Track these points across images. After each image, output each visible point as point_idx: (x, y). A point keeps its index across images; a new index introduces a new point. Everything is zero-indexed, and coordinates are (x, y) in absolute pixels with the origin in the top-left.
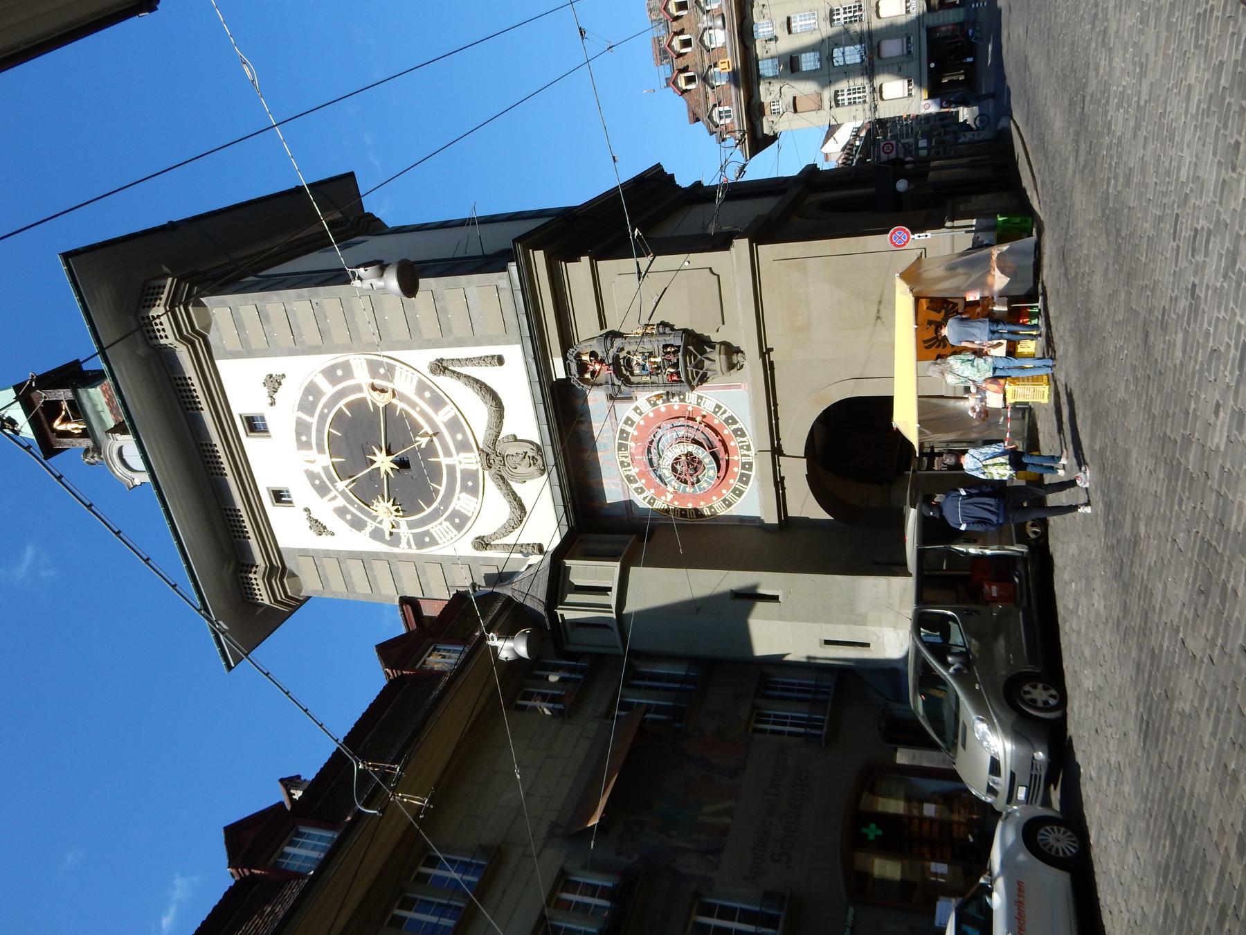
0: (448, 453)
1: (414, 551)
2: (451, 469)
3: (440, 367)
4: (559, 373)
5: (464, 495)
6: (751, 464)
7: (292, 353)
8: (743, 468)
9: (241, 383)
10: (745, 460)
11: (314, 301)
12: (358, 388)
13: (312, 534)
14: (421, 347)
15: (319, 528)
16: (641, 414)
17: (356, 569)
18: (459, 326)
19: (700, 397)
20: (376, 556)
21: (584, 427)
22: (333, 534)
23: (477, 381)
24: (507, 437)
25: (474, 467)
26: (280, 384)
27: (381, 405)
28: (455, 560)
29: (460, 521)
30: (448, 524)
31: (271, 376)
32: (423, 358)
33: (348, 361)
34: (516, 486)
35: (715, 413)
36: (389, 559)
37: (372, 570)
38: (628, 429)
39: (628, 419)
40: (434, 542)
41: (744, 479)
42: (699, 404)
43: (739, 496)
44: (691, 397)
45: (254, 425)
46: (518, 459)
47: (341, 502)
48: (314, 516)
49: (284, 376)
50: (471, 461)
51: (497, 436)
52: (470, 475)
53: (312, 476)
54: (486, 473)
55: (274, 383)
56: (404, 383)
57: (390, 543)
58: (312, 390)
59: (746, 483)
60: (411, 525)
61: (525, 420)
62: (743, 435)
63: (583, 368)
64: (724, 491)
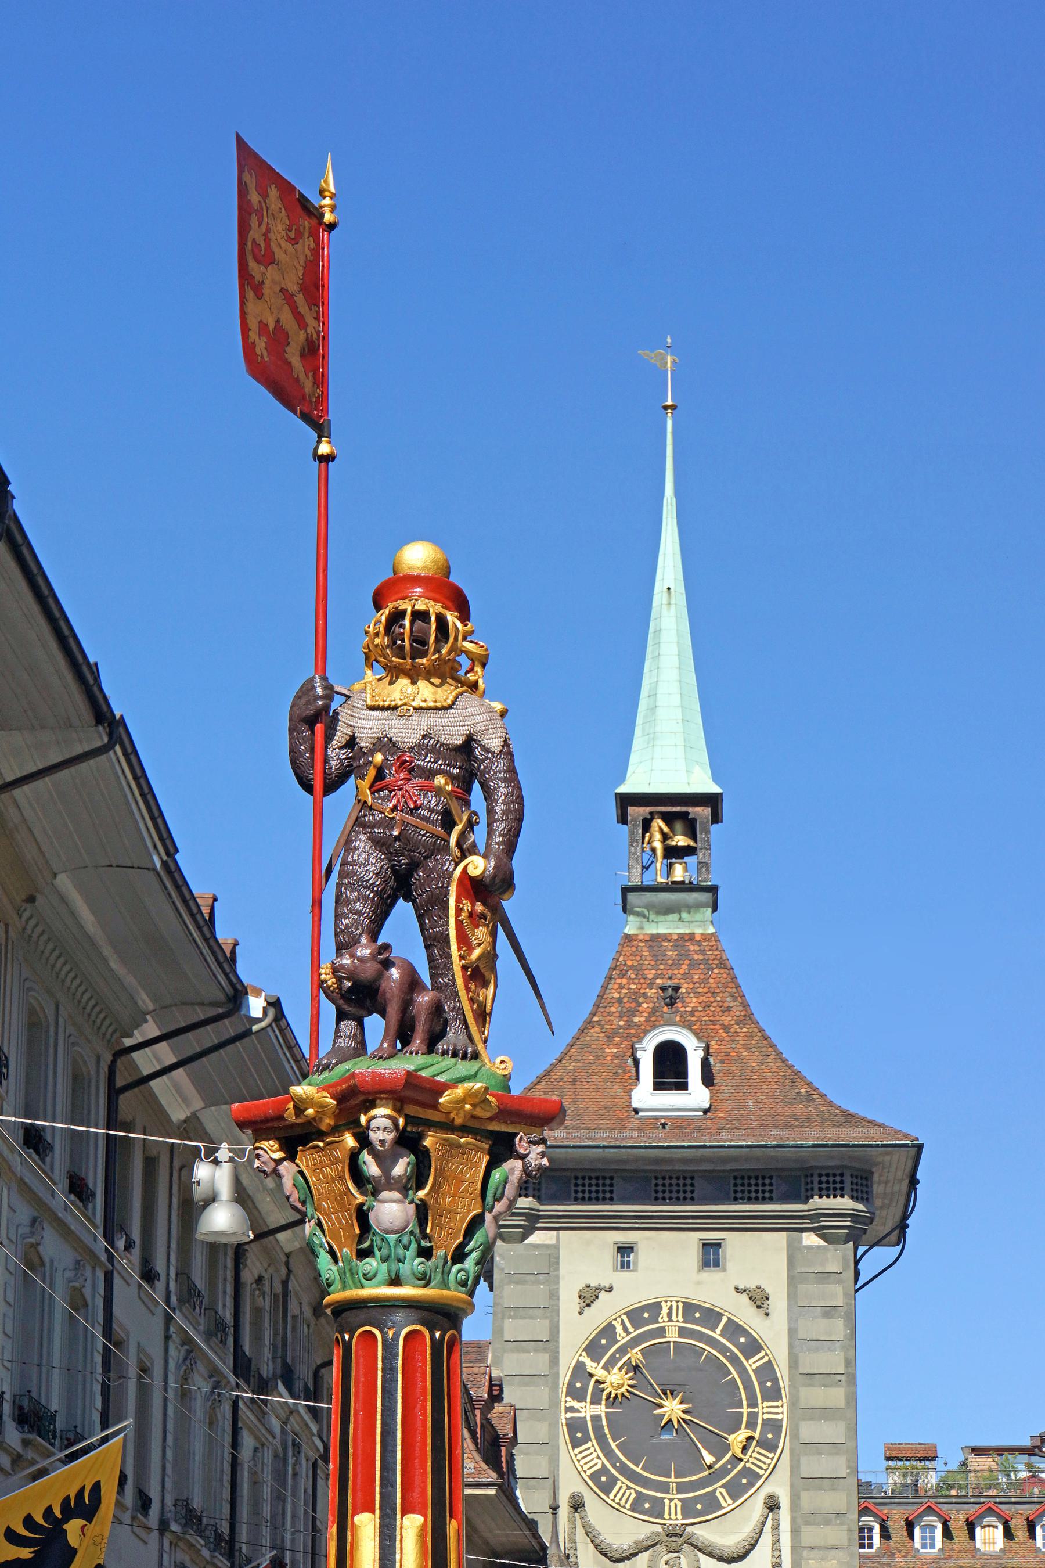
0: (681, 1488)
1: (564, 1416)
2: (665, 1488)
3: (772, 1506)
7: (792, 1332)
9: (759, 1256)
11: (843, 1378)
12: (753, 1404)
14: (792, 1486)
15: (588, 1297)
17: (539, 1329)
18: (810, 1535)
20: (555, 1361)
23: (757, 1541)
26: (759, 1307)
28: (554, 1462)
30: (599, 1466)
31: (768, 1299)
32: (779, 1486)
33: (779, 1397)
36: (550, 1377)
37: (536, 1351)
40: (575, 1443)
45: (711, 1255)
47: (622, 1338)
48: (603, 1295)
49: (767, 1314)
50: (674, 1516)
51: (700, 1550)
52: (657, 1510)
53: (655, 1308)
54: (659, 1529)
55: (759, 1300)
57: (571, 1386)
58: (753, 1347)
60: (596, 1419)
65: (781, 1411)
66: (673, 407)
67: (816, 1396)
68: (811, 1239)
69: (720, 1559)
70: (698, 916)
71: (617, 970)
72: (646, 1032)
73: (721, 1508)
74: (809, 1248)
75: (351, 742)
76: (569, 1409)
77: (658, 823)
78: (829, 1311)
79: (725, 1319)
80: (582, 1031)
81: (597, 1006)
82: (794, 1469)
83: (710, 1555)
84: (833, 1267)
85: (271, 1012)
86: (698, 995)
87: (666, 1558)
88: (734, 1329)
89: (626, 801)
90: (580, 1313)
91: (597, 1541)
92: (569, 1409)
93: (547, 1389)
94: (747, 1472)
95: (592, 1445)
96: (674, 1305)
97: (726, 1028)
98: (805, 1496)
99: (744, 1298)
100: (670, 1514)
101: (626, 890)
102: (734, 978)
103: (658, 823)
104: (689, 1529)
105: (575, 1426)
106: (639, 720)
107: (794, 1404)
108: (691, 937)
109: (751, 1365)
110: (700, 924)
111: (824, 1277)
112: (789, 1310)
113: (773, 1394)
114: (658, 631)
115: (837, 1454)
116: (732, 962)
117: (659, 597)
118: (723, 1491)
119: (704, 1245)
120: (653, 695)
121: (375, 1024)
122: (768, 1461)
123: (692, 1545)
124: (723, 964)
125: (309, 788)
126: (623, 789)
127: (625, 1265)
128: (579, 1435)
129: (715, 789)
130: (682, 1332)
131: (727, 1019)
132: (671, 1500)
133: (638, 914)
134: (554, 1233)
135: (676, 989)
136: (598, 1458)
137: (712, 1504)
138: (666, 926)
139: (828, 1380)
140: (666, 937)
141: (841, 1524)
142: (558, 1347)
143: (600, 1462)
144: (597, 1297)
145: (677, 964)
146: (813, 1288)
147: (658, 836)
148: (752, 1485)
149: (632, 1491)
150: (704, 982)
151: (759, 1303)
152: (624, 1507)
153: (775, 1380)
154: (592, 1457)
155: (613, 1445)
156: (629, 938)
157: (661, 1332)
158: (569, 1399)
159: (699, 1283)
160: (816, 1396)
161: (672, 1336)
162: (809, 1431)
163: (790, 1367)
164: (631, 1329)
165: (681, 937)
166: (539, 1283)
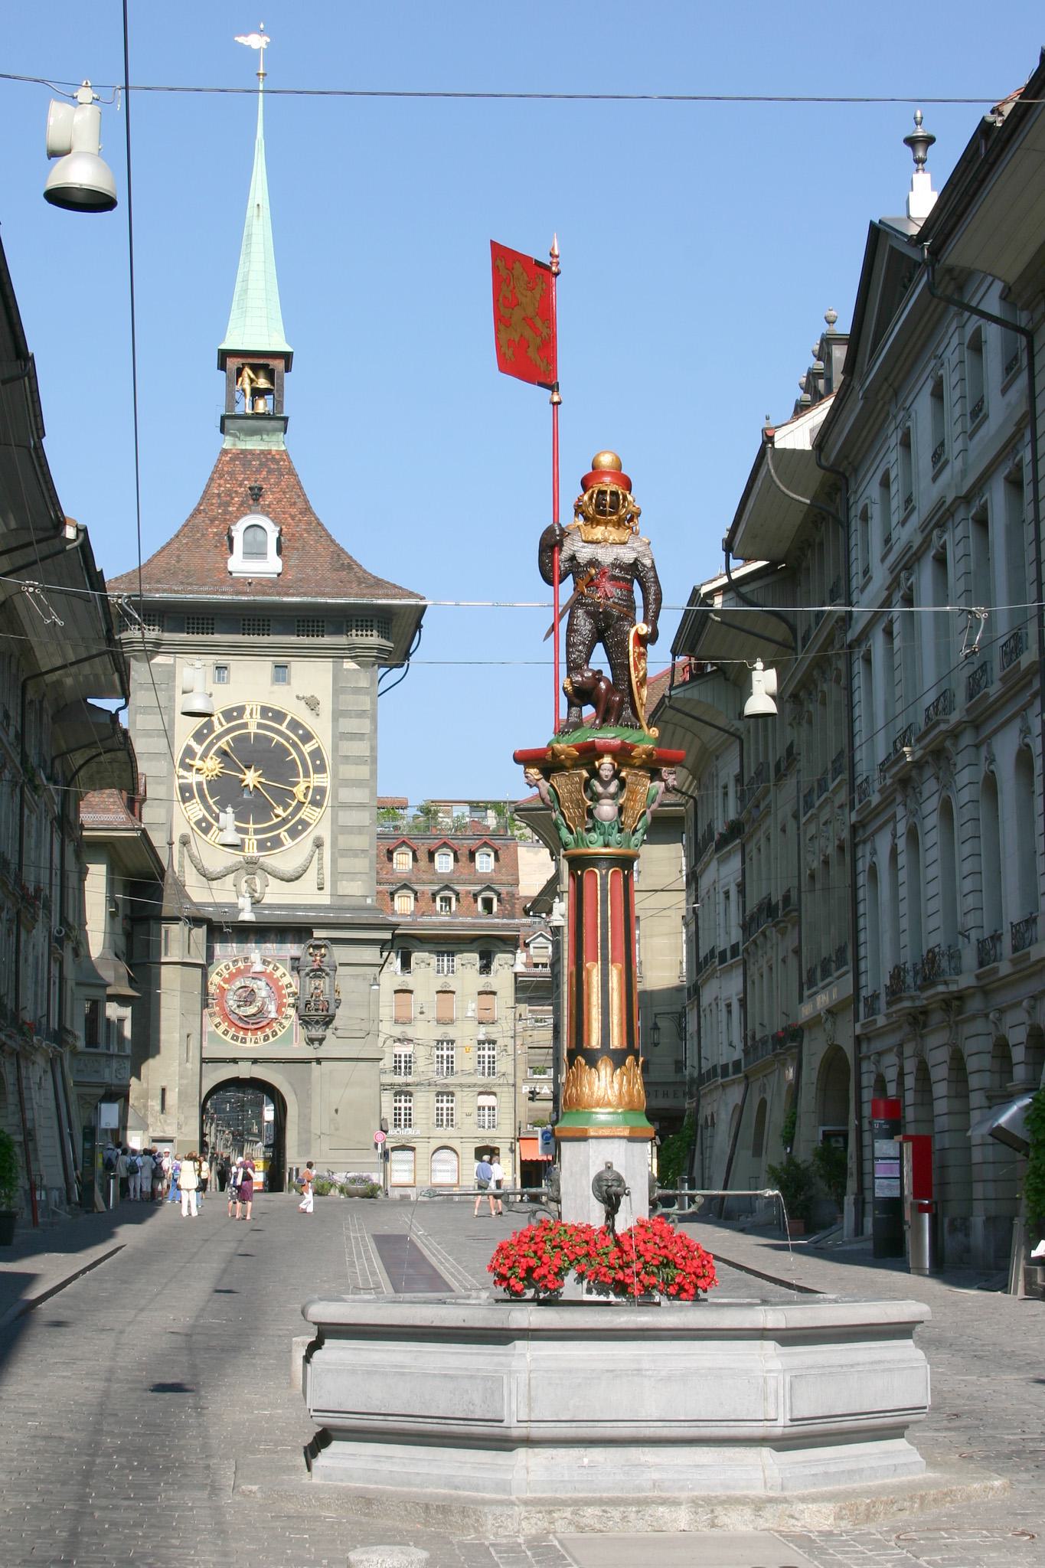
0: (257, 832)
1: (177, 782)
4: (317, 934)
14: (332, 832)
18: (344, 864)
20: (170, 746)
21: (273, 937)
27: (295, 790)
29: (204, 826)
32: (324, 831)
33: (325, 771)
34: (231, 877)
41: (235, 1038)
44: (292, 1012)
47: (218, 729)
50: (251, 851)
53: (241, 710)
55: (312, 704)
58: (307, 737)
63: (318, 947)
65: (324, 780)
66: (264, 75)
67: (350, 771)
68: (350, 665)
69: (282, 879)
70: (274, 438)
71: (218, 473)
72: (238, 518)
73: (283, 845)
75: (573, 558)
77: (247, 371)
78: (361, 714)
79: (288, 718)
80: (192, 516)
81: (203, 498)
82: (334, 820)
84: (364, 683)
85: (82, 535)
86: (273, 493)
88: (295, 725)
89: (224, 355)
94: (301, 821)
97: (293, 517)
98: (340, 838)
101: (223, 418)
102: (299, 483)
103: (247, 371)
105: (185, 789)
106: (236, 298)
107: (335, 776)
108: (269, 452)
109: (307, 749)
110: (273, 443)
111: (357, 691)
112: (333, 712)
113: (320, 769)
114: (250, 236)
116: (298, 471)
117: (251, 210)
120: (245, 281)
121: (588, 711)
124: (291, 472)
125: (549, 581)
126: (223, 347)
127: (220, 680)
129: (287, 349)
130: (260, 726)
131: (293, 511)
133: (234, 435)
135: (260, 489)
137: (277, 842)
138: (253, 444)
139: (359, 760)
140: (251, 452)
145: (259, 471)
146: (350, 698)
147: (247, 381)
148: (304, 830)
150: (278, 484)
153: (322, 760)
154: (196, 810)
155: (211, 802)
156: (225, 452)
157: (245, 726)
160: (350, 771)
161: (253, 729)
165: (262, 452)
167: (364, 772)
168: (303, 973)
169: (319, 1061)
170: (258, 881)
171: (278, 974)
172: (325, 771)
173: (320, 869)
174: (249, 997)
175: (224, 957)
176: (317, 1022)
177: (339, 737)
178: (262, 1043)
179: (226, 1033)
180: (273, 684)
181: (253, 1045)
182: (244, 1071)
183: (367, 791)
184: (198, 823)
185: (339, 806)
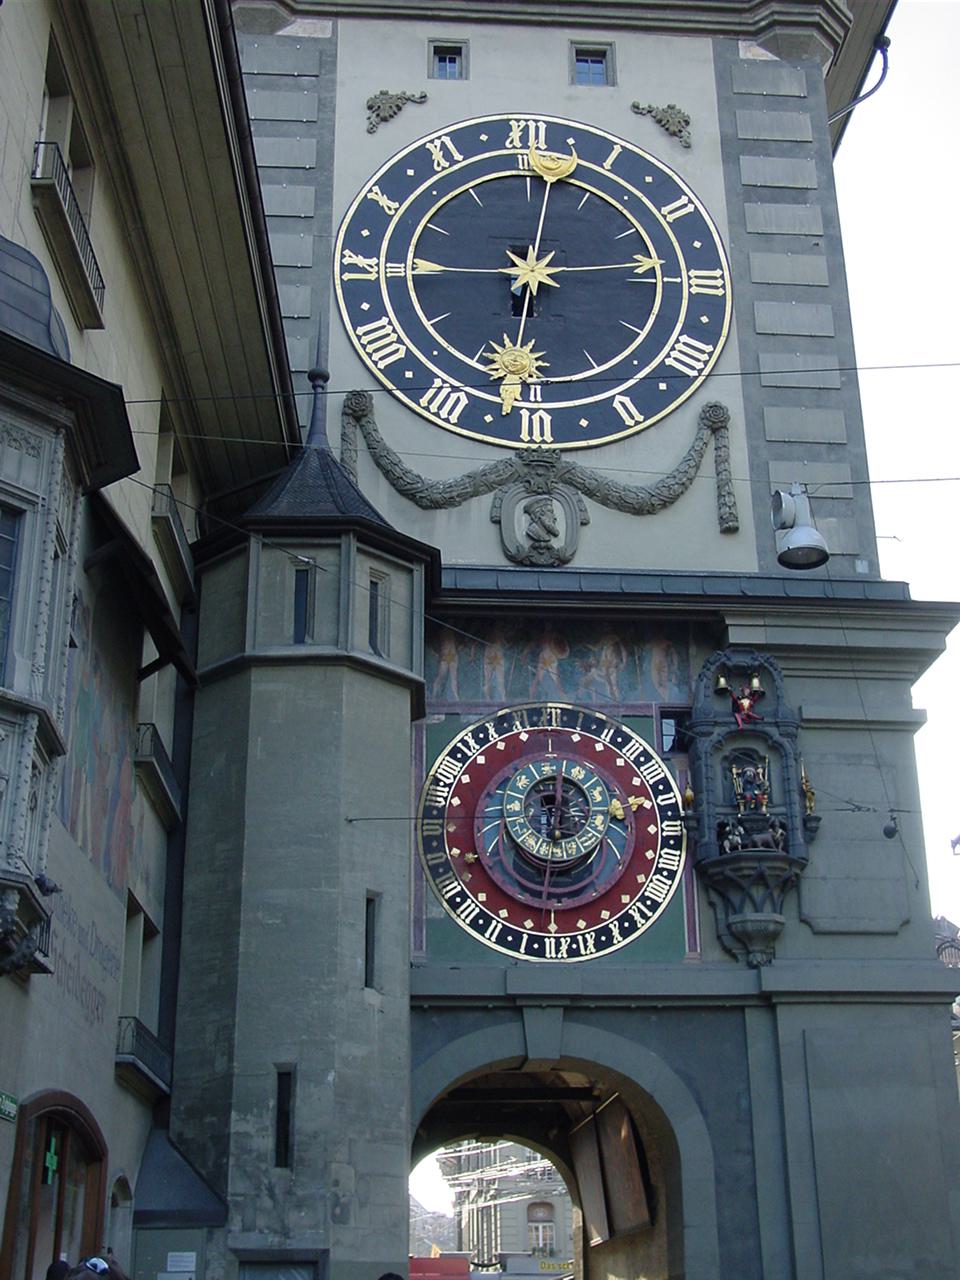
5: (464, 401)
6: (541, 953)
8: (532, 939)
10: (550, 943)
11: (821, 242)
12: (671, 268)
13: (374, 91)
14: (747, 398)
15: (384, 110)
16: (637, 761)
17: (302, 150)
19: (672, 875)
20: (324, 196)
21: (607, 654)
22: (370, 131)
24: (584, 511)
25: (525, 435)
26: (674, 134)
28: (319, 349)
29: (410, 380)
30: (401, 354)
32: (728, 393)
33: (718, 265)
34: (482, 505)
35: (643, 899)
36: (317, 220)
37: (291, 182)
38: (606, 736)
39: (627, 739)
42: (659, 871)
43: (474, 924)
46: (548, 522)
47: (442, 168)
49: (688, 146)
51: (590, 493)
52: (508, 424)
54: (513, 452)
55: (673, 125)
56: (680, 351)
58: (665, 189)
59: (501, 941)
60: (397, 285)
61: (606, 549)
62: (599, 946)
64: (482, 897)
68: (750, 51)
74: (752, 63)
76: (345, 269)
79: (617, 150)
83: (605, 501)
87: (524, 503)
88: (632, 164)
90: (370, 131)
91: (398, 472)
92: (345, 269)
93: (310, 239)
94: (665, 372)
95: (389, 324)
96: (532, 125)
99: (648, 123)
100: (531, 433)
104: (565, 457)
105: (360, 293)
107: (741, 274)
109: (667, 215)
111: (776, 101)
112: (725, 142)
113: (706, 259)
115: (822, 352)
118: (627, 400)
119: (579, 53)
122: (705, 357)
123: (570, 483)
128: (365, 306)
132: (532, 411)
134: (328, 24)
136: (399, 341)
141: (839, 461)
142: (330, 179)
143: (403, 349)
144: (400, 109)
149: (462, 395)
151: (672, 129)
152: (447, 420)
158: (347, 252)
159: (570, 98)
162: (771, 316)
163: (730, 222)
164: (458, 156)
166: (301, 89)
167: (811, 268)
168: (704, 745)
169: (768, 1001)
170: (557, 507)
171: (629, 753)
172: (718, 265)
173: (723, 490)
174: (555, 805)
175: (471, 707)
176: (761, 879)
177: (742, 194)
178: (589, 953)
179: (481, 923)
180: (573, 82)
181: (569, 955)
182: (546, 1040)
183: (826, 312)
184: (393, 371)
185: (758, 339)
